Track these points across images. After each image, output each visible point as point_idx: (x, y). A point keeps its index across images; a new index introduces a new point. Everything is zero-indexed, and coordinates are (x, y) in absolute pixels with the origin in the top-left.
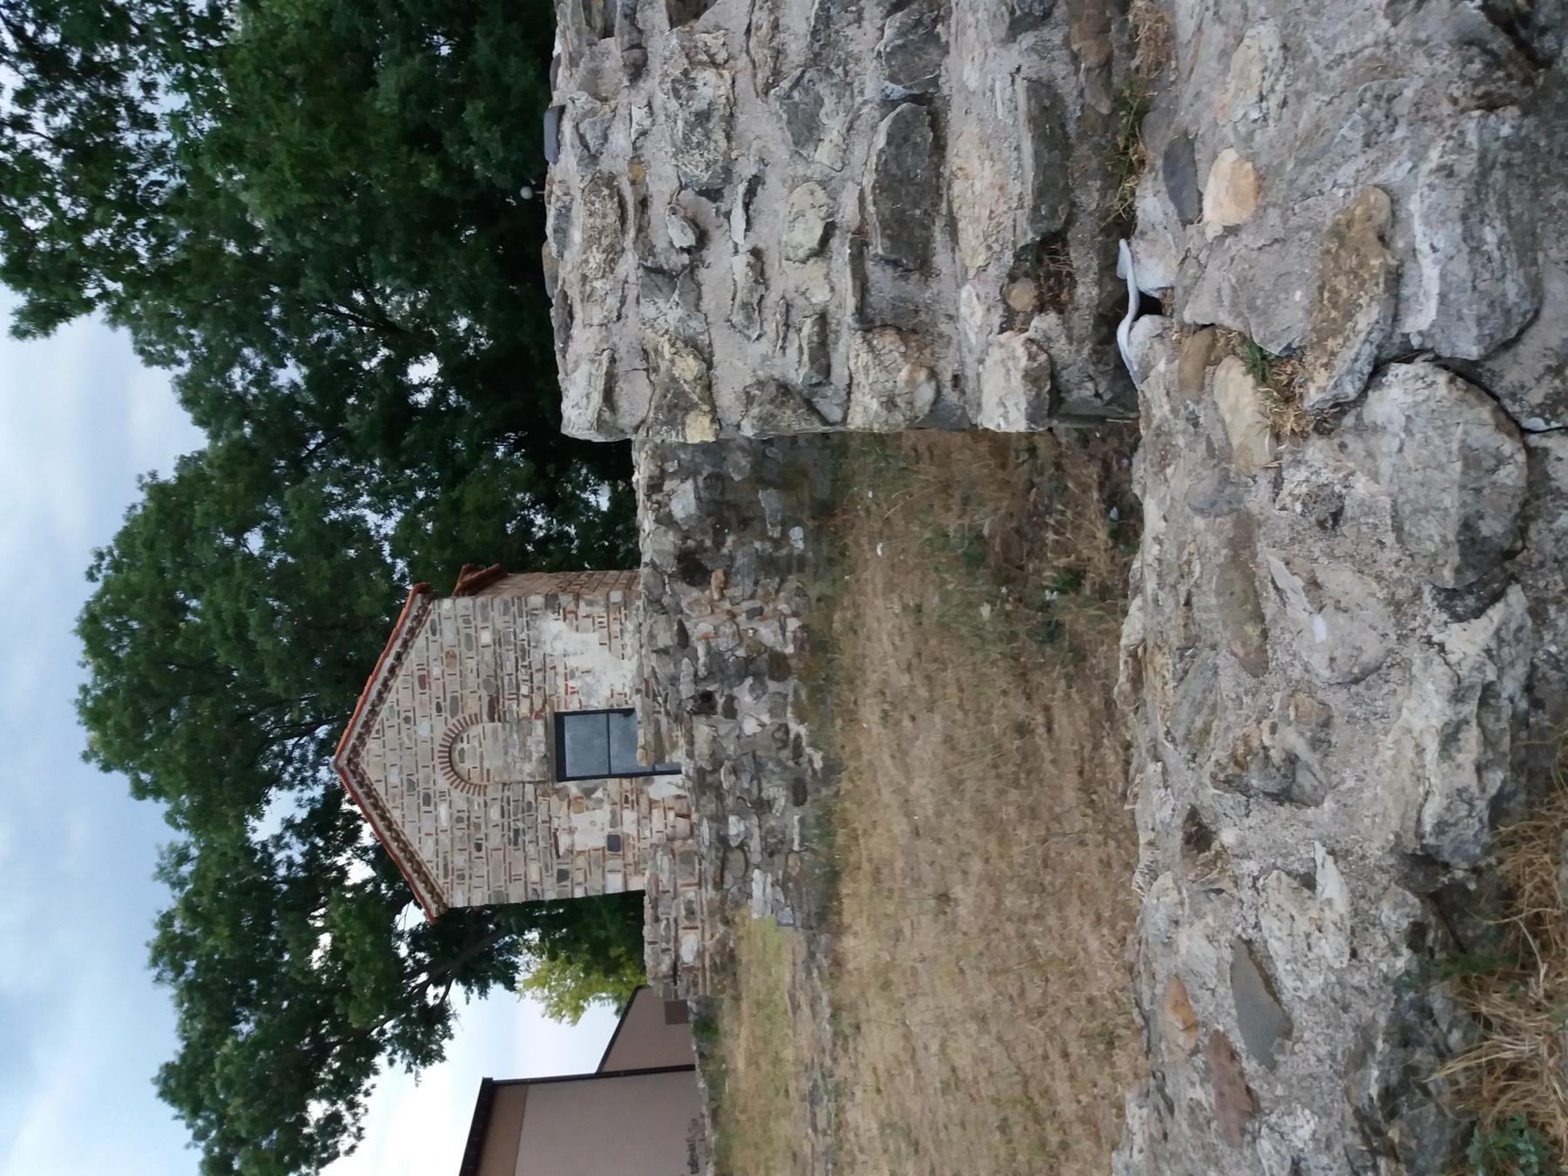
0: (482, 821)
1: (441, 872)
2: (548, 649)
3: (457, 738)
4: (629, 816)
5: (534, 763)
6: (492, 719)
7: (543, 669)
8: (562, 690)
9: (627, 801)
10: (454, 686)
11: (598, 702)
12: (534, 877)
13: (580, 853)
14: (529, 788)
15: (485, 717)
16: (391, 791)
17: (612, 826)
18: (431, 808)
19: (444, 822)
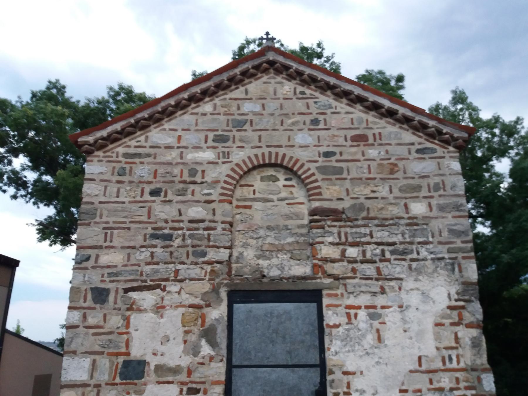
0: (189, 197)
1: (132, 151)
2: (409, 284)
3: (291, 172)
5: (254, 262)
6: (313, 212)
7: (380, 277)
8: (351, 301)
11: (337, 352)
13: (127, 320)
15: (316, 204)
17: (159, 368)
18: (210, 143)
19: (190, 156)
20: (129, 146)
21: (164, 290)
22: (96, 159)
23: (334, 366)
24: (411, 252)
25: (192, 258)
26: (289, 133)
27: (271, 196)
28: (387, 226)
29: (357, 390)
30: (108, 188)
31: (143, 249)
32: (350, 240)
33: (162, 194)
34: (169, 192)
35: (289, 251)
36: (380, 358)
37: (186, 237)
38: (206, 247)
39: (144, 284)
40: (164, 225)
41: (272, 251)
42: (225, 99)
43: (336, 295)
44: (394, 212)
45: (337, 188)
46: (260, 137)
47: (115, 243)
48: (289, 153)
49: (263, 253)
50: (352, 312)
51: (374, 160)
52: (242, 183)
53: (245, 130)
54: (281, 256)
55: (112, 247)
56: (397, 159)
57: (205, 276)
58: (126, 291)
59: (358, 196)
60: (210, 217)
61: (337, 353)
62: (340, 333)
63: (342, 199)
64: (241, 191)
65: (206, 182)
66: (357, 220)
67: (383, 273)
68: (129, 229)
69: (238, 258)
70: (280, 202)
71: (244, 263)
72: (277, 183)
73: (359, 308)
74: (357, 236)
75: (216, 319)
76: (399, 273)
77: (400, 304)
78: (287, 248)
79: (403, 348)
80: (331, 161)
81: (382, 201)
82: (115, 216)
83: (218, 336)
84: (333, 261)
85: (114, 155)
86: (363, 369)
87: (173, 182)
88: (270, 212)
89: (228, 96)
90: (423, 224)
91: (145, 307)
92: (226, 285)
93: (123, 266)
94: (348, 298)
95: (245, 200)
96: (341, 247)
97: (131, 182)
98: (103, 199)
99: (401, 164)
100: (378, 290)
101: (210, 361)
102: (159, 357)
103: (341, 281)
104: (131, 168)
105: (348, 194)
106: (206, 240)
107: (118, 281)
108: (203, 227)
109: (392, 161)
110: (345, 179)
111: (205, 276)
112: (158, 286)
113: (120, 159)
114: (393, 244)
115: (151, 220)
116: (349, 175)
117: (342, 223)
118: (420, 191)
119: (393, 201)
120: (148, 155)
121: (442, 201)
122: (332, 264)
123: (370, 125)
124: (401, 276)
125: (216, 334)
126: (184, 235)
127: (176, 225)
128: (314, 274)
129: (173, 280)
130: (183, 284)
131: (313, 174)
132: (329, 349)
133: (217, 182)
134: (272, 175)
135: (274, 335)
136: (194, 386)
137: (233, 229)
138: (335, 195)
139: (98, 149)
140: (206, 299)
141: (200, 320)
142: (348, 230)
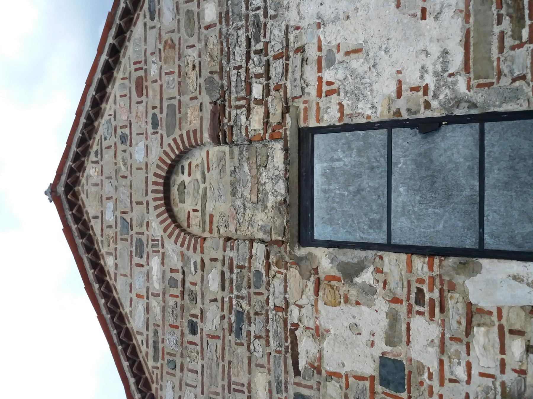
2: (292, 17)
3: (173, 167)
4: (424, 330)
7: (283, 56)
8: (312, 90)
9: (420, 301)
11: (373, 107)
13: (332, 375)
14: (259, 250)
15: (206, 136)
16: (107, 231)
20: (147, 354)
21: (297, 326)
22: (159, 392)
23: (389, 109)
24: (256, 16)
25: (262, 290)
26: (134, 169)
27: (200, 191)
28: (229, 48)
29: (422, 77)
30: (188, 382)
31: (252, 347)
32: (243, 94)
33: (195, 320)
34: (193, 312)
35: (258, 170)
36: (380, 47)
37: (239, 294)
38: (250, 271)
39: (290, 351)
40: (226, 320)
41: (258, 191)
42: (102, 241)
43: (306, 109)
44: (215, 42)
45: (189, 111)
46: (138, 203)
47: (245, 381)
48: (153, 169)
49: (261, 203)
50: (325, 88)
51: (161, 68)
52: (185, 225)
53: (131, 219)
55: (249, 384)
56: (160, 42)
57: (282, 273)
58: (297, 373)
59: (198, 85)
60: (219, 264)
61: (373, 107)
62: (350, 103)
63: (201, 104)
64: (195, 227)
65: (182, 267)
66: (222, 86)
67: (280, 51)
68: (230, 362)
69: (265, 233)
70: (207, 180)
71: (271, 224)
72: (186, 184)
73: (320, 79)
74: (239, 85)
75: (332, 262)
76: (280, 31)
77: (315, 26)
78: (254, 171)
79: (368, 19)
80: (161, 118)
81: (203, 57)
82: (216, 377)
83: (351, 261)
84: (267, 115)
85: (156, 371)
86: (394, 70)
87: (182, 306)
88: (216, 192)
89: (100, 239)
90: (227, 5)
91: (316, 351)
92: (292, 248)
93: (270, 374)
94: (309, 94)
95: (204, 222)
96: (252, 105)
97: (182, 356)
98: (199, 389)
99: (165, 37)
100: (299, 56)
101: (382, 272)
102: (376, 339)
103: (290, 104)
104: (168, 354)
105: (196, 98)
106: (243, 271)
107: (286, 382)
108: (229, 273)
109: (161, 47)
110: (180, 101)
111: (282, 273)
112: (293, 332)
113: (159, 365)
114: (248, 40)
115: (221, 335)
116: (175, 98)
117: (227, 103)
118: (192, 11)
119: (203, 43)
120: (156, 333)
122: (271, 115)
123: (127, 75)
124: (284, 27)
125: (348, 264)
126: (238, 297)
127: (226, 306)
128: (281, 138)
129: (286, 314)
130: (291, 301)
131: (175, 140)
132: (369, 117)
133: (182, 255)
134: (178, 190)
135: (351, 189)
136: (413, 296)
137: (235, 238)
138: (197, 113)
139: (150, 389)
140: (308, 273)
141: (333, 283)
142: (233, 96)
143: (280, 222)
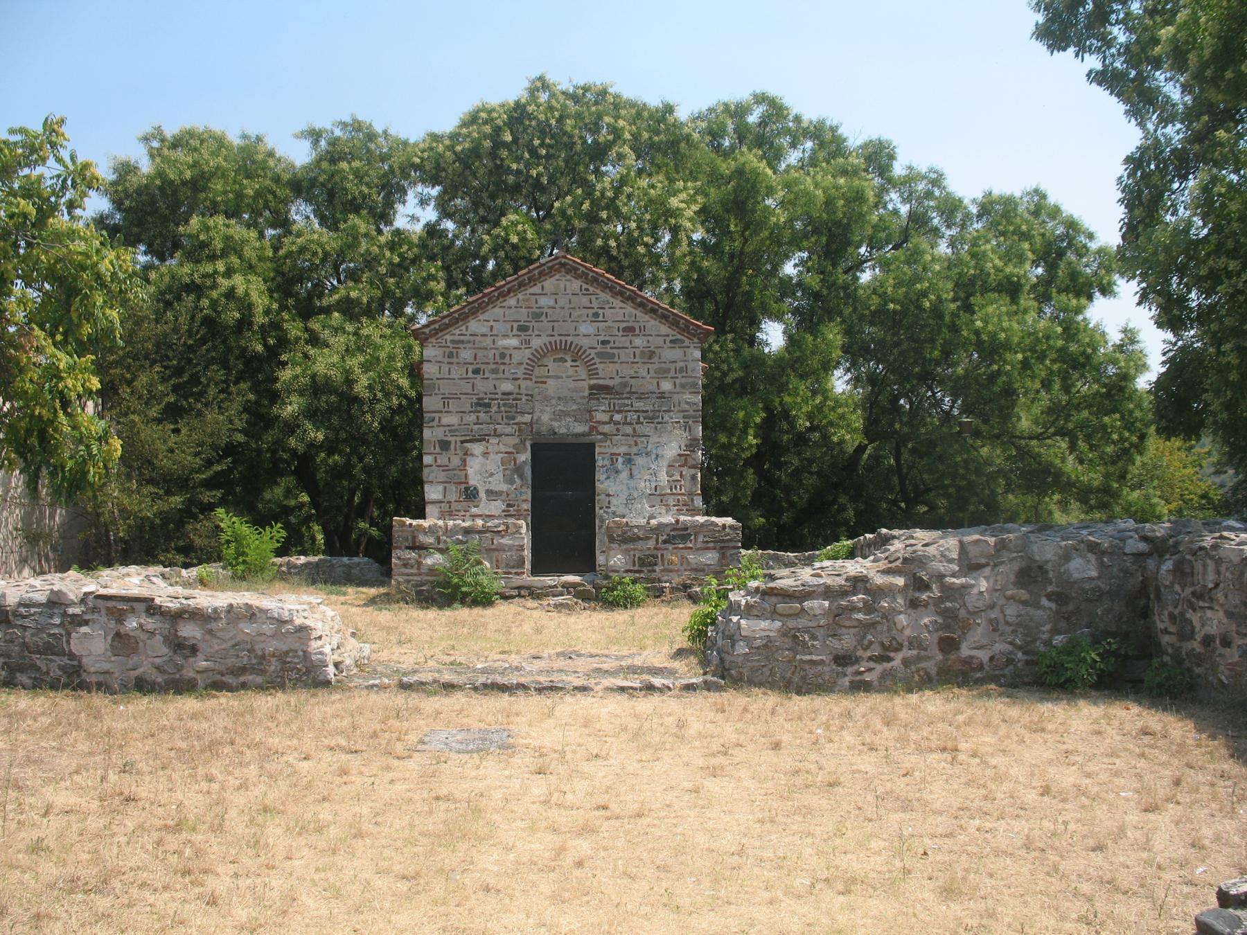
0: (501, 375)
1: (457, 338)
6: (592, 387)
8: (615, 450)
9: (509, 506)
10: (625, 355)
12: (446, 420)
13: (464, 461)
14: (527, 418)
15: (593, 382)
18: (515, 332)
19: (503, 343)
48: (576, 340)
54: (568, 419)
58: (462, 442)
84: (604, 423)
121: (684, 381)
139: (432, 336)
143: (544, 429)
